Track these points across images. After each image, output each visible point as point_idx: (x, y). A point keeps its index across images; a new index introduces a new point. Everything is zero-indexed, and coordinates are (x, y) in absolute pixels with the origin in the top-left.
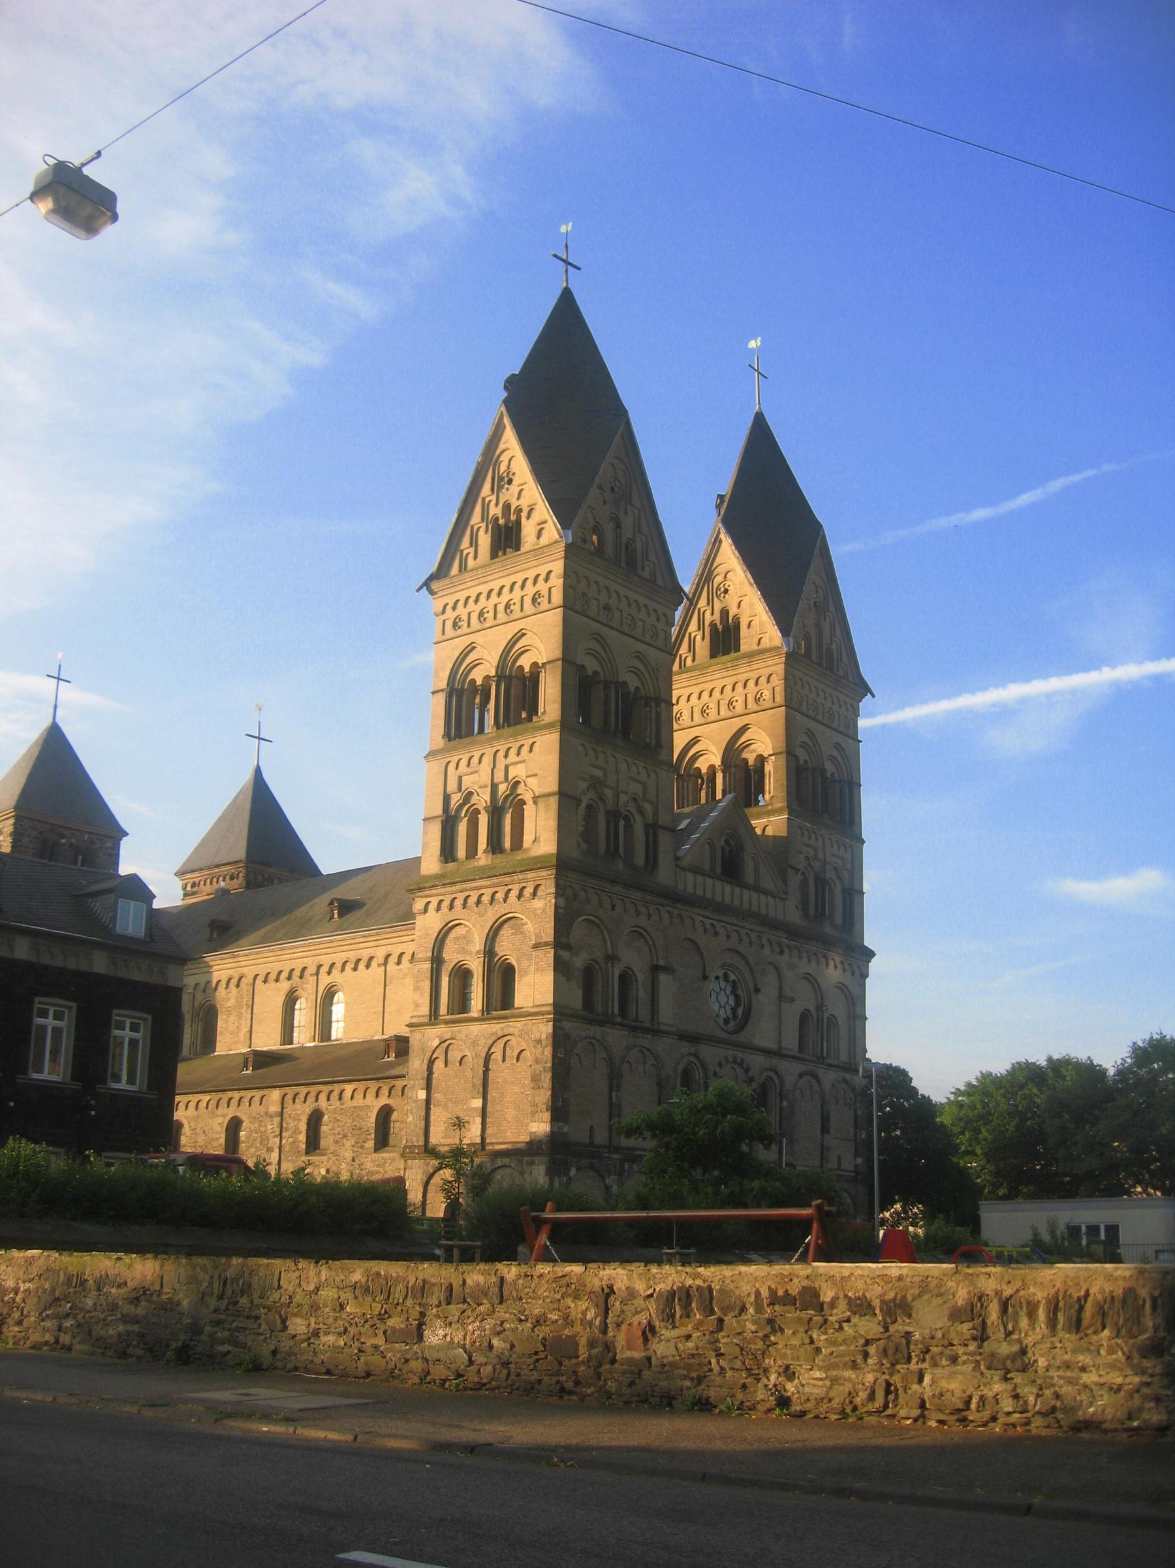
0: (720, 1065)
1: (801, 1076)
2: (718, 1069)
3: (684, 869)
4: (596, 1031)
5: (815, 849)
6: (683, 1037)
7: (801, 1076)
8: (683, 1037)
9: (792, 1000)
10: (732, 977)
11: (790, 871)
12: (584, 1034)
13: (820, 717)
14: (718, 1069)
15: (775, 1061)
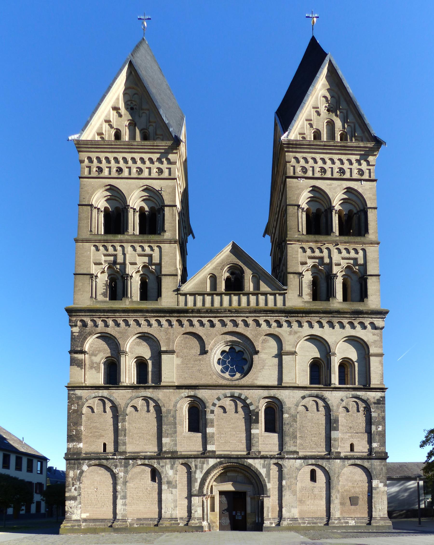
0: (219, 399)
1: (303, 398)
2: (216, 402)
3: (185, 295)
4: (105, 393)
5: (321, 259)
6: (179, 387)
7: (303, 398)
8: (179, 387)
9: (294, 353)
10: (237, 349)
11: (290, 276)
12: (94, 395)
13: (328, 175)
14: (216, 402)
15: (273, 393)
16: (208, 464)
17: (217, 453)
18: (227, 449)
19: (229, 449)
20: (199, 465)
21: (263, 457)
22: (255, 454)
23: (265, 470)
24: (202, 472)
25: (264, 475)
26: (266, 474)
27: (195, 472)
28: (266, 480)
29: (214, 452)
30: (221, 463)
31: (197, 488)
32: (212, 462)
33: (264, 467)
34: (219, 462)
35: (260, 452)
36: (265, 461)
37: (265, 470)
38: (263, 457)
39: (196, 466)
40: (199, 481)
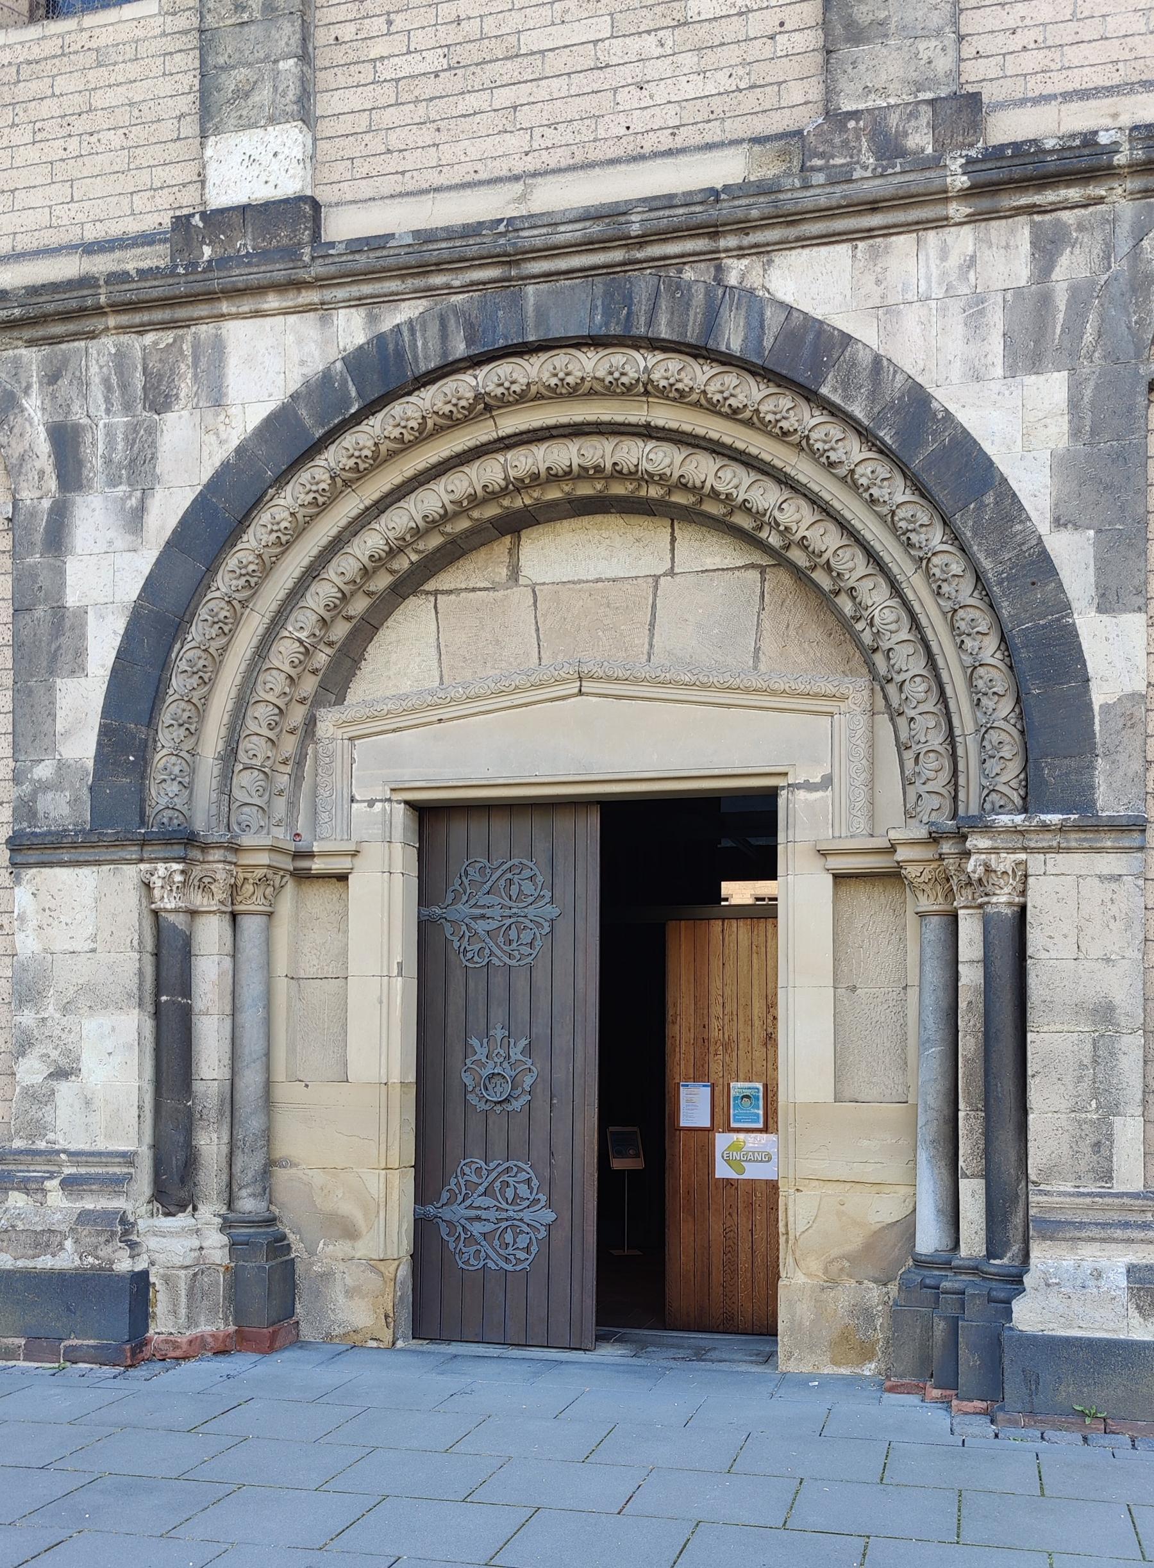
16: (218, 402)
17: (342, 226)
18: (471, 152)
19: (510, 151)
20: (103, 424)
21: (1016, 179)
22: (889, 148)
23: (1051, 389)
24: (135, 519)
25: (1033, 483)
26: (1062, 464)
27: (57, 536)
28: (1073, 556)
29: (305, 211)
30: (383, 375)
31: (81, 745)
32: (269, 359)
33: (1028, 353)
34: (355, 361)
35: (965, 109)
36: (1047, 249)
37: (1051, 389)
38: (1016, 179)
39: (66, 441)
40: (103, 643)
